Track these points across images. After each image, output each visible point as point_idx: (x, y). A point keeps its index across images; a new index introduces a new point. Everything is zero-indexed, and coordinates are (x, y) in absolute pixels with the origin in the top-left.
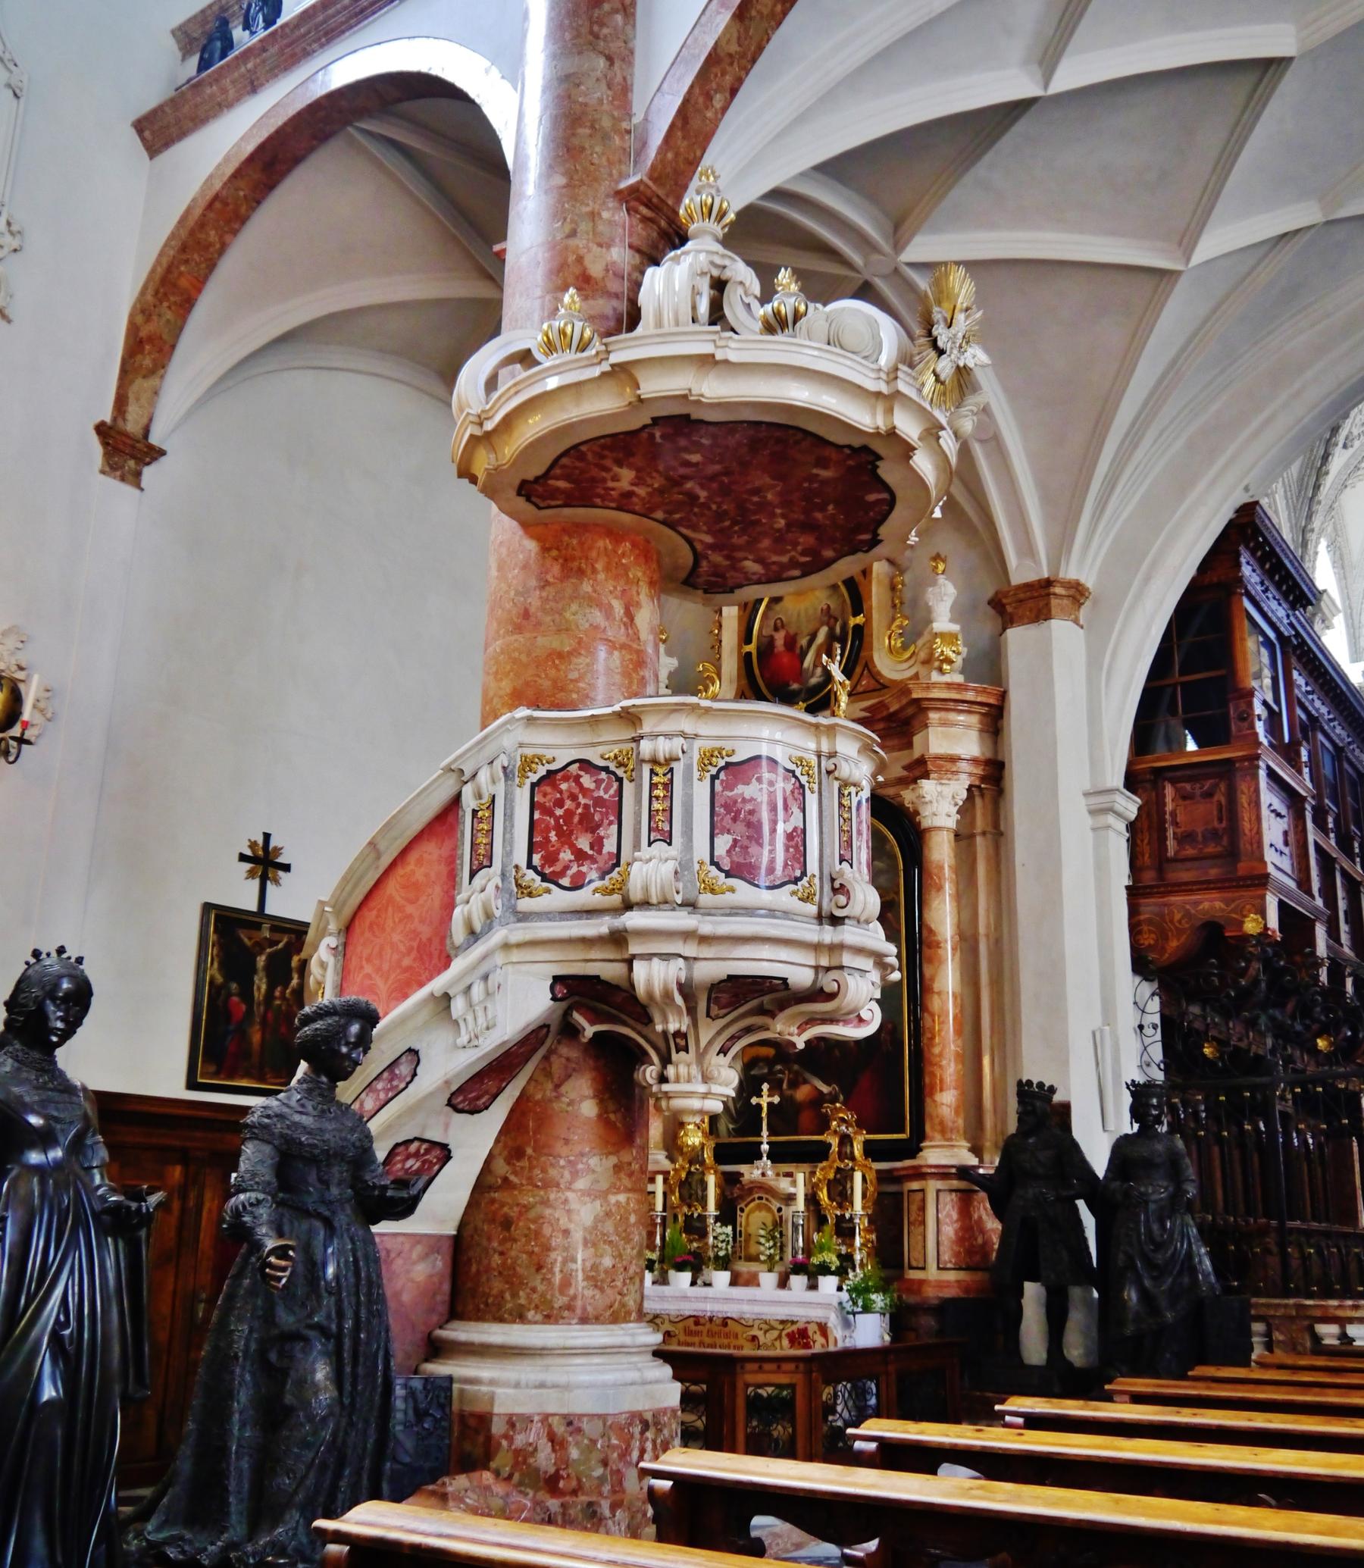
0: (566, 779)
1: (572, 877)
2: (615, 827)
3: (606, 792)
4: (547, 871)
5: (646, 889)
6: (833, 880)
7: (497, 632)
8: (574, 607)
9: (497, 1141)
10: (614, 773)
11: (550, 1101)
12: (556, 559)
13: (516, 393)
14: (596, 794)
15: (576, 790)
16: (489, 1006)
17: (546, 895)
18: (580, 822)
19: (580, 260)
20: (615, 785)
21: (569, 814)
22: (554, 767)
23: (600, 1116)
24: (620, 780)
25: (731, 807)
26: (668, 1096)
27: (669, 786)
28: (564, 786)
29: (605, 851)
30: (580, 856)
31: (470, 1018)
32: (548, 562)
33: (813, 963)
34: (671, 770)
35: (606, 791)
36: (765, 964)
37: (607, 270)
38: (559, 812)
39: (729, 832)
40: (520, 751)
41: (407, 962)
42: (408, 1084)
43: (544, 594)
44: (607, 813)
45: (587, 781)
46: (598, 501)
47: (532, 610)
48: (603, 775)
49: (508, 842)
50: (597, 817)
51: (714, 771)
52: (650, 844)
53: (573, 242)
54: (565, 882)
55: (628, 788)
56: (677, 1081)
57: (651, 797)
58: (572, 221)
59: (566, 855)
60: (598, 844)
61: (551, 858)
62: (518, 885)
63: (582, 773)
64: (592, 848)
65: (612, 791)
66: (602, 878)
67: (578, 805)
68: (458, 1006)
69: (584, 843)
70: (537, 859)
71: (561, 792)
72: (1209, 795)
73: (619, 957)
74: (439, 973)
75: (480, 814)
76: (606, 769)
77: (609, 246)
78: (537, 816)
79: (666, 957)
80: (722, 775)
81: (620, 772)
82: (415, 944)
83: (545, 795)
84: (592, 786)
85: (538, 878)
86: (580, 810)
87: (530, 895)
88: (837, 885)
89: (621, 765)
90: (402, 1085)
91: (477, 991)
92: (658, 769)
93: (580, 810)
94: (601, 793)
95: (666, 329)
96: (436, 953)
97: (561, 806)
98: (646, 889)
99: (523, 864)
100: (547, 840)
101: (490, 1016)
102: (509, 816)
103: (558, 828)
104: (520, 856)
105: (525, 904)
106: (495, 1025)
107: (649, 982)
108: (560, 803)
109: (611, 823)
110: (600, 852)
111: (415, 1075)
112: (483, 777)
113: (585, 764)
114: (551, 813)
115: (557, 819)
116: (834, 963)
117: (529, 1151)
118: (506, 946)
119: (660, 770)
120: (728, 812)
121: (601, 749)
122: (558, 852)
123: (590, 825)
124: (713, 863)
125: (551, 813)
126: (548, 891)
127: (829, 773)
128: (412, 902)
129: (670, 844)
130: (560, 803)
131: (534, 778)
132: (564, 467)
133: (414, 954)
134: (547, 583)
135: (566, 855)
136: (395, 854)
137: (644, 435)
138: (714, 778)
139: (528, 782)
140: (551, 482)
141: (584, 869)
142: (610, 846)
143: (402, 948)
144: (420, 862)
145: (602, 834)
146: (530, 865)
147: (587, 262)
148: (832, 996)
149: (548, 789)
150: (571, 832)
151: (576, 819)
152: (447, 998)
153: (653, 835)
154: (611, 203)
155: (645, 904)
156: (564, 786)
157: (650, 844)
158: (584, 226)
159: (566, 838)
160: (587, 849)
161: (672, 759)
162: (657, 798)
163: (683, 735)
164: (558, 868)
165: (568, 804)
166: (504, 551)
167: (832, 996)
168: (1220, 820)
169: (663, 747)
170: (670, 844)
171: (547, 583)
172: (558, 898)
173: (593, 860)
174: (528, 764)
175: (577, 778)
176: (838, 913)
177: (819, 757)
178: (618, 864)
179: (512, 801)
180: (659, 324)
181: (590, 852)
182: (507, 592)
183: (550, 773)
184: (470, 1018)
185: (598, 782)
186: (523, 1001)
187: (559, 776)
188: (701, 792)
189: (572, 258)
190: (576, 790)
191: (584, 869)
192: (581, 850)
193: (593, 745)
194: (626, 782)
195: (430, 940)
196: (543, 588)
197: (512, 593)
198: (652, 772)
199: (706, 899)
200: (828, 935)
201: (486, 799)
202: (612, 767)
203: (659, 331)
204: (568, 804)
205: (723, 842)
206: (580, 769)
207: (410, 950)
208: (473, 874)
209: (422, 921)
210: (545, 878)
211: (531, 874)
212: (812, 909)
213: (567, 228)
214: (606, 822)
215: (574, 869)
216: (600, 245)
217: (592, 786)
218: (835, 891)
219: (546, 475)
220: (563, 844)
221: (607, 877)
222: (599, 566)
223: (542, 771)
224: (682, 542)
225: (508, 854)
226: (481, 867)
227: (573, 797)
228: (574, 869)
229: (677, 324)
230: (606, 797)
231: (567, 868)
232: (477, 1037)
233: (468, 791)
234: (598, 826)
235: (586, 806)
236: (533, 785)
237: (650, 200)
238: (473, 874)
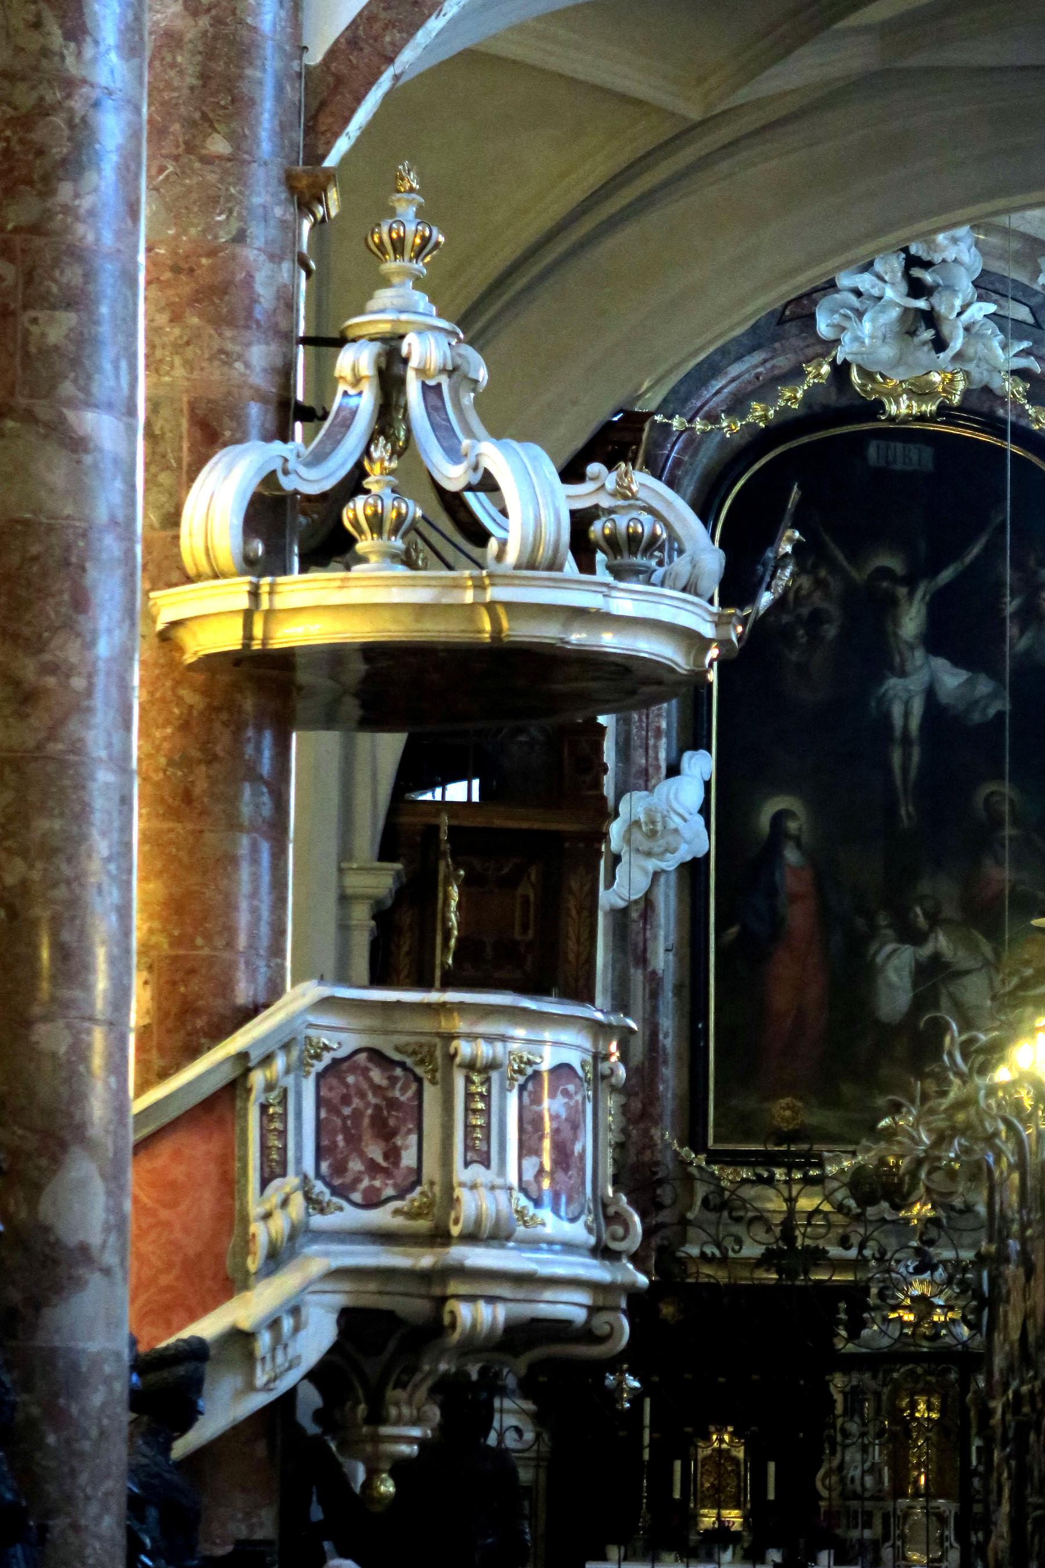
0: (354, 1069)
2: (413, 1138)
6: (605, 1206)
14: (390, 1094)
15: (365, 1086)
17: (338, 1213)
20: (414, 1087)
21: (357, 1115)
22: (341, 1054)
24: (419, 1080)
27: (486, 1098)
28: (351, 1079)
30: (373, 1168)
32: (217, 726)
35: (404, 1090)
41: (164, 1280)
44: (404, 1121)
45: (377, 1075)
47: (197, 791)
48: (398, 1072)
50: (392, 1122)
51: (521, 1079)
54: (357, 1197)
55: (431, 1094)
56: (399, 1421)
60: (393, 1154)
61: (340, 1168)
63: (370, 1065)
65: (410, 1093)
66: (400, 1196)
70: (324, 1166)
71: (347, 1086)
72: (510, 883)
73: (423, 1291)
75: (271, 1111)
76: (402, 1065)
79: (491, 1299)
81: (419, 1071)
82: (177, 1259)
83: (331, 1089)
84: (384, 1083)
85: (327, 1191)
87: (322, 1211)
88: (611, 1210)
89: (422, 1062)
92: (476, 1078)
94: (397, 1093)
99: (311, 1173)
100: (335, 1143)
103: (345, 1130)
109: (409, 1132)
110: (396, 1162)
113: (376, 1055)
114: (338, 1113)
115: (344, 1119)
119: (476, 1078)
123: (386, 1133)
124: (523, 1189)
125: (338, 1113)
126: (341, 1209)
127: (604, 1077)
129: (488, 1166)
133: (176, 1271)
135: (356, 1165)
138: (522, 1088)
142: (408, 1159)
144: (177, 1155)
145: (399, 1143)
146: (318, 1175)
149: (334, 1082)
155: (471, 1237)
156: (351, 1079)
159: (354, 1141)
160: (380, 1159)
162: (475, 1111)
164: (348, 1178)
165: (356, 1102)
168: (525, 927)
169: (484, 1051)
170: (488, 1166)
172: (349, 1216)
175: (365, 1071)
176: (615, 1246)
181: (384, 1164)
183: (336, 1062)
185: (393, 1080)
187: (345, 1065)
191: (377, 1183)
192: (372, 1160)
193: (386, 1032)
194: (426, 1084)
195: (199, 1256)
197: (163, 761)
198: (469, 1081)
202: (409, 1061)
204: (356, 1102)
207: (170, 1266)
208: (264, 1183)
210: (335, 1191)
213: (235, 226)
214: (403, 1130)
215: (366, 1183)
217: (384, 1083)
221: (409, 1197)
223: (327, 1058)
225: (299, 1161)
226: (273, 1176)
227: (362, 1095)
228: (366, 1183)
230: (403, 1099)
231: (357, 1180)
233: (258, 1079)
235: (377, 1107)
236: (320, 1076)
238: (264, 1183)
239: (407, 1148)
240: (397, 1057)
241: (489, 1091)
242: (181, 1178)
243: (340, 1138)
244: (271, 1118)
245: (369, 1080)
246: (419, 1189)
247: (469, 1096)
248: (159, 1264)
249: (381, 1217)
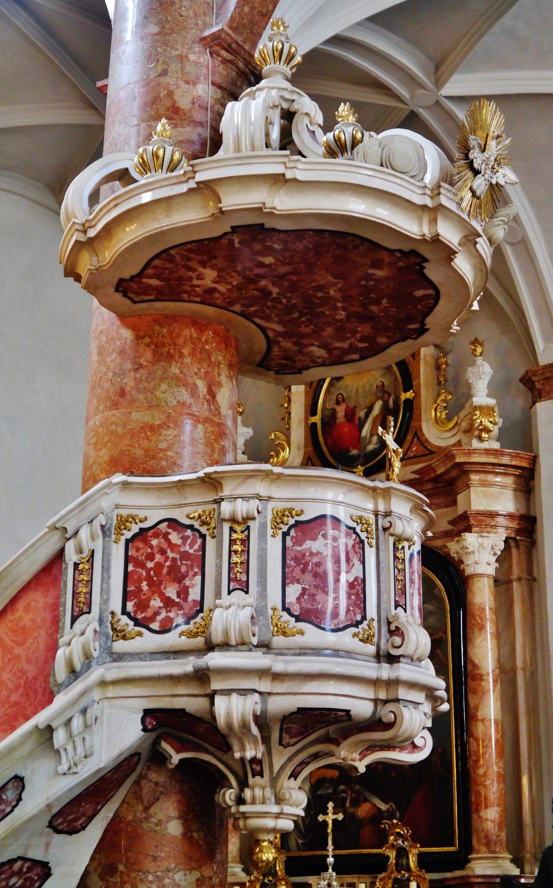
0: (156, 536)
1: (162, 622)
2: (198, 578)
3: (191, 548)
4: (140, 616)
5: (226, 633)
6: (389, 623)
7: (97, 408)
8: (164, 387)
9: (92, 858)
10: (198, 531)
11: (141, 821)
12: (148, 345)
13: (116, 206)
14: (182, 549)
15: (165, 546)
16: (87, 737)
17: (138, 638)
18: (169, 573)
19: (170, 94)
20: (199, 541)
21: (159, 566)
22: (145, 525)
23: (184, 835)
24: (203, 537)
25: (299, 559)
26: (245, 816)
27: (246, 542)
28: (154, 542)
29: (190, 598)
30: (168, 603)
31: (70, 748)
32: (142, 348)
33: (372, 696)
34: (248, 528)
35: (191, 546)
36: (331, 698)
37: (193, 103)
38: (150, 565)
39: (298, 582)
40: (116, 512)
41: (14, 698)
42: (14, 808)
43: (138, 375)
44: (192, 566)
45: (174, 537)
46: (185, 296)
47: (128, 389)
48: (189, 532)
49: (105, 591)
50: (183, 569)
51: (285, 528)
52: (229, 593)
53: (165, 80)
54: (155, 626)
55: (210, 543)
56: (253, 802)
57: (230, 552)
58: (164, 63)
59: (156, 603)
60: (184, 593)
61: (143, 606)
62: (114, 629)
63: (170, 531)
64: (178, 596)
65: (196, 547)
66: (187, 623)
67: (167, 558)
68: (60, 737)
69: (171, 592)
70: (130, 606)
71: (152, 547)
73: (202, 693)
74: (43, 708)
75: (81, 566)
76: (191, 527)
77: (195, 84)
78: (130, 568)
79: (243, 692)
80: (292, 532)
81: (203, 530)
82: (22, 682)
83: (138, 550)
84: (179, 542)
85: (131, 623)
86: (168, 563)
87: (124, 638)
88: (393, 627)
89: (204, 523)
90: (8, 809)
91: (77, 723)
93: (168, 563)
94: (187, 548)
95: (244, 153)
96: (40, 690)
97: (152, 560)
98: (226, 633)
99: (118, 610)
100: (139, 589)
101: (88, 746)
102: (106, 569)
103: (149, 579)
104: (116, 604)
105: (120, 646)
106: (92, 754)
107: (229, 715)
108: (150, 557)
109: (195, 574)
110: (185, 599)
111: (19, 799)
112: (84, 534)
113: (173, 523)
114: (142, 565)
115: (148, 571)
116: (390, 697)
117: (121, 868)
118: (103, 684)
119: (238, 528)
120: (298, 565)
121: (187, 510)
122: (149, 600)
123: (177, 576)
124: (284, 609)
125: (142, 565)
126: (140, 634)
127: (385, 529)
128: (20, 644)
129: (247, 592)
130: (150, 557)
131: (128, 535)
132: (155, 267)
133: (21, 690)
134: (141, 366)
135: (156, 603)
136: (6, 602)
137: (225, 241)
138: (285, 535)
139: (123, 539)
140: (144, 280)
141: (172, 615)
142: (194, 594)
143: (11, 686)
144: (27, 608)
145: (187, 583)
146: (124, 612)
147: (177, 96)
148: (390, 726)
149: (141, 545)
150: (161, 583)
151: (165, 571)
152: (50, 730)
153: (232, 584)
154: (197, 48)
155: (225, 646)
156: (154, 542)
157: (229, 593)
158: (174, 67)
159: (156, 587)
160: (174, 597)
161: (249, 518)
162: (236, 552)
163: (258, 497)
164: (149, 613)
165: (158, 558)
166: (103, 338)
167: (390, 726)
169: (241, 508)
170: (247, 592)
171: (141, 366)
172: (149, 641)
173: (180, 608)
174: (123, 522)
175: (166, 536)
176: (394, 652)
177: (376, 515)
178: (201, 610)
179: (109, 555)
180: (238, 149)
181: (177, 600)
182: (106, 374)
183: (142, 531)
184: (70, 748)
185: (184, 539)
186: (119, 732)
187: (150, 533)
188: (274, 547)
189: (163, 93)
190: (165, 546)
191: (172, 615)
192: (169, 597)
193: (180, 506)
194: (208, 538)
195: (35, 678)
196: (136, 370)
198: (232, 530)
199: (278, 641)
200: (386, 671)
201: (86, 554)
202: (197, 525)
203: (238, 155)
204: (158, 558)
205: (293, 591)
206: (169, 527)
207: (18, 687)
208: (74, 619)
209: (29, 661)
210: (137, 623)
211: (125, 619)
212: (371, 649)
213: (160, 69)
214: (191, 573)
215: (163, 615)
216: (187, 82)
217: (179, 542)
218: (391, 633)
219: (141, 274)
220: (153, 593)
221: (192, 622)
222: (185, 351)
223: (135, 529)
224: (258, 330)
225: (105, 601)
226: (81, 613)
227: (163, 552)
228: (163, 615)
229: (253, 149)
230: (191, 551)
231: (157, 613)
232: (76, 765)
233: (70, 547)
234: (184, 577)
235: (174, 560)
236: (128, 541)
237: (230, 46)
238: (74, 619)
239: (193, 586)
240: (187, 522)
241: (248, 537)
242: (29, 624)
243: (144, 584)
244: (81, 572)
245: (168, 541)
246: (201, 615)
247: (232, 542)
248: (13, 688)
249: (172, 639)
